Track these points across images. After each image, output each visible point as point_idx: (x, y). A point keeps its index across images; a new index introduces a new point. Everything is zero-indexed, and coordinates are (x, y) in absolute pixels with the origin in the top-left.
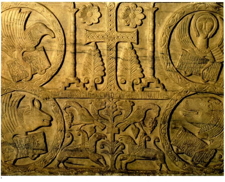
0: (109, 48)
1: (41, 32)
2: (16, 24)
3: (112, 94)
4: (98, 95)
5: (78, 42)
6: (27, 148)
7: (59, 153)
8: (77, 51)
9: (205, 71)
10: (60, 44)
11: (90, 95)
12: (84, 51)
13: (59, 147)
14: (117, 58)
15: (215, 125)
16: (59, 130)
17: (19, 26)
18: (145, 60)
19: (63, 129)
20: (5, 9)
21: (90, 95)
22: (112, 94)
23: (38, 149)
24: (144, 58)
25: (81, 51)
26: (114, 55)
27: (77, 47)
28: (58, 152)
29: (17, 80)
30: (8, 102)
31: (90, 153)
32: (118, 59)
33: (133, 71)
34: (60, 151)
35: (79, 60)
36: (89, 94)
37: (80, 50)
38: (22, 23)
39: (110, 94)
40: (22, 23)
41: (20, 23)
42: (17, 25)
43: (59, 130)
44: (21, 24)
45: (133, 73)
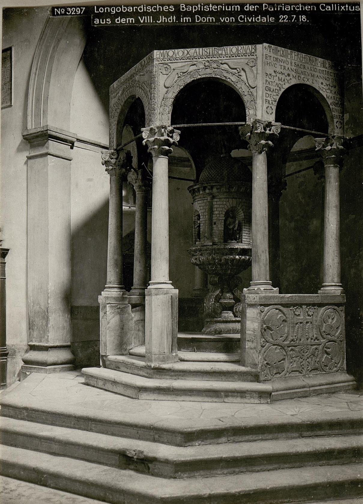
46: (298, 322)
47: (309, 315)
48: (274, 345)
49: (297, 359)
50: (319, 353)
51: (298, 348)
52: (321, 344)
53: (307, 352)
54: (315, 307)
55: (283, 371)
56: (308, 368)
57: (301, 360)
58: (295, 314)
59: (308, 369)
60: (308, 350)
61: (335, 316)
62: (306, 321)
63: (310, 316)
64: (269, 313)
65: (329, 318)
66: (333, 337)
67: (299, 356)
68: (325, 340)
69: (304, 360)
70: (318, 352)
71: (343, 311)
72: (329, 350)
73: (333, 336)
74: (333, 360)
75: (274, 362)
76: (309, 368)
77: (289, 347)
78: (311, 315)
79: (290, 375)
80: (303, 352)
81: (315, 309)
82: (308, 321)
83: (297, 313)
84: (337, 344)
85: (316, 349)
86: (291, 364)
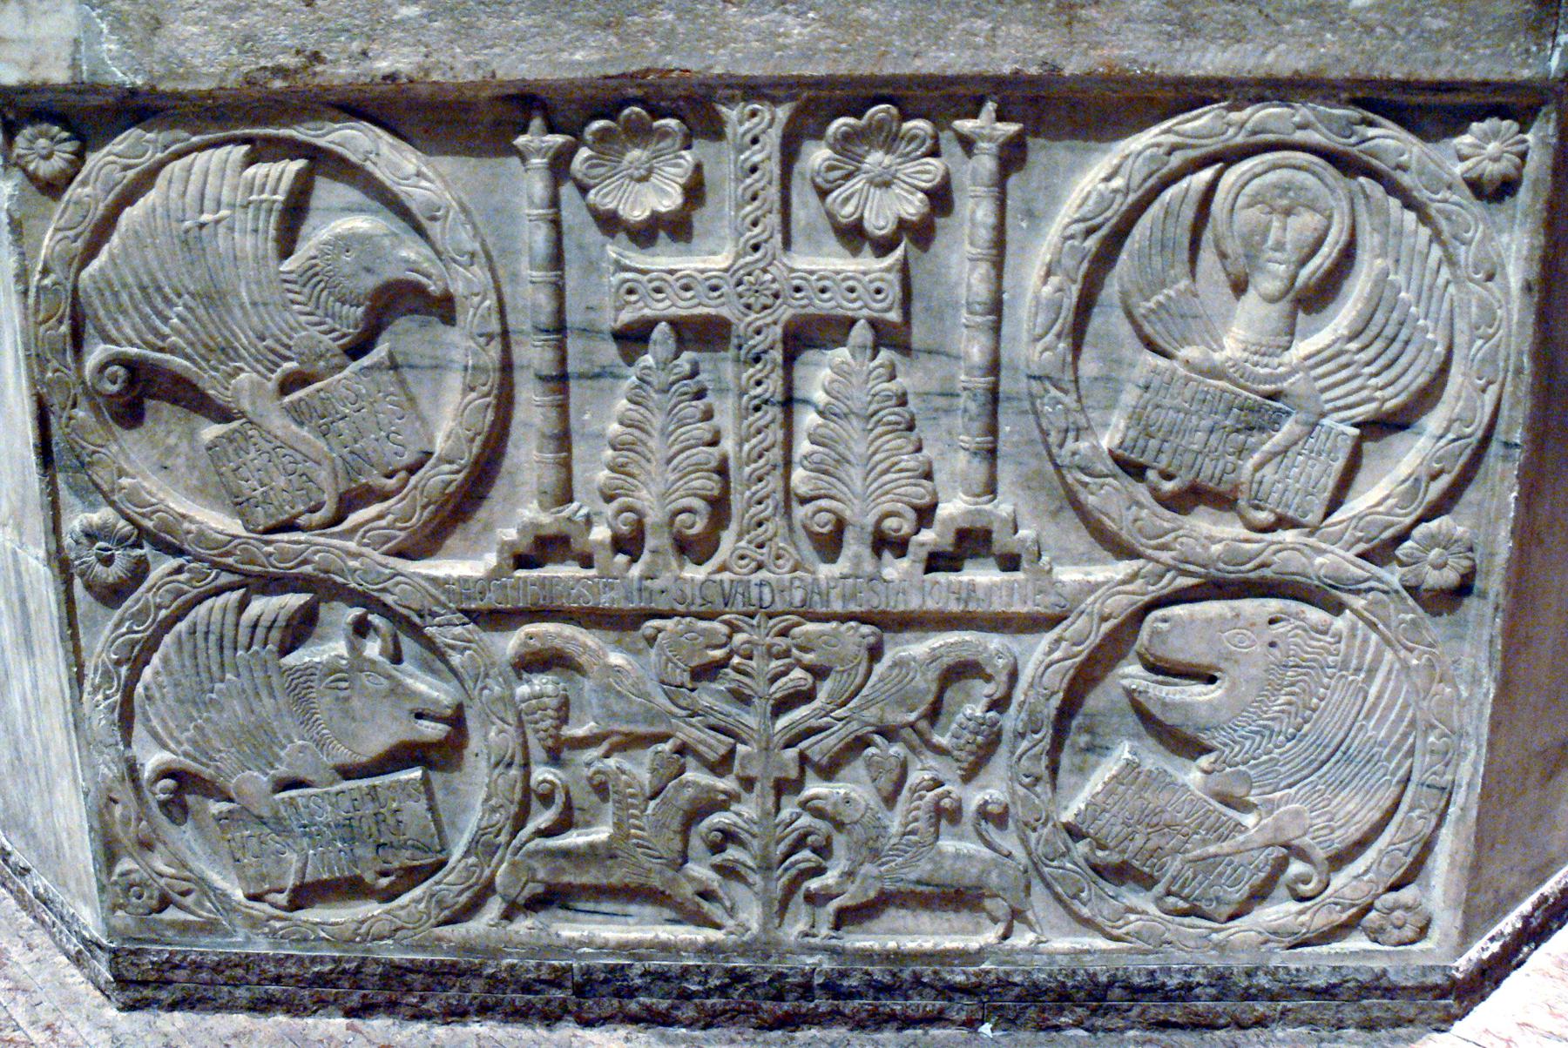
0: (743, 352)
1: (368, 270)
2: (231, 229)
3: (766, 590)
4: (688, 592)
5: (574, 317)
6: (350, 840)
7: (505, 865)
8: (572, 367)
9: (1268, 470)
10: (476, 331)
11: (645, 594)
12: (616, 370)
13: (503, 838)
14: (789, 403)
15: (1294, 737)
16: (497, 765)
17: (249, 241)
18: (948, 411)
19: (518, 759)
20: (166, 147)
21: (645, 594)
22: (766, 590)
23: (404, 846)
24: (942, 402)
25: (597, 370)
26: (773, 386)
27: (574, 345)
28: (501, 862)
29: (263, 523)
30: (229, 632)
31: (655, 864)
32: (797, 407)
33: (879, 468)
34: (508, 856)
35: (583, 417)
36: (640, 590)
37: (591, 362)
38: (261, 225)
39: (754, 592)
40: (261, 225)
41: (250, 226)
42: (237, 235)
43: (497, 765)
44: (256, 231)
45: (875, 480)
46: (651, 324)
47: (853, 235)
48: (273, 584)
49: (638, 769)
50: (1011, 720)
51: (651, 640)
52: (1051, 622)
53: (807, 696)
54: (966, 125)
55: (413, 876)
56: (819, 871)
57: (695, 775)
58: (609, 223)
59: (814, 884)
60: (819, 673)
61: (1348, 254)
62: (785, 313)
63: (883, 247)
64: (151, 197)
65: (1239, 287)
66: (1289, 536)
67: (664, 738)
68: (1124, 568)
69: (748, 783)
70: (999, 705)
71: (1524, 195)
72: (1195, 693)
73: (1282, 523)
74: (1249, 820)
75: (282, 770)
76: (830, 878)
77: (498, 619)
78: (879, 222)
79: (523, 926)
80: (741, 698)
81: (967, 143)
82: (824, 305)
83: (639, 205)
84: (1340, 623)
85: (961, 671)
86: (543, 818)
